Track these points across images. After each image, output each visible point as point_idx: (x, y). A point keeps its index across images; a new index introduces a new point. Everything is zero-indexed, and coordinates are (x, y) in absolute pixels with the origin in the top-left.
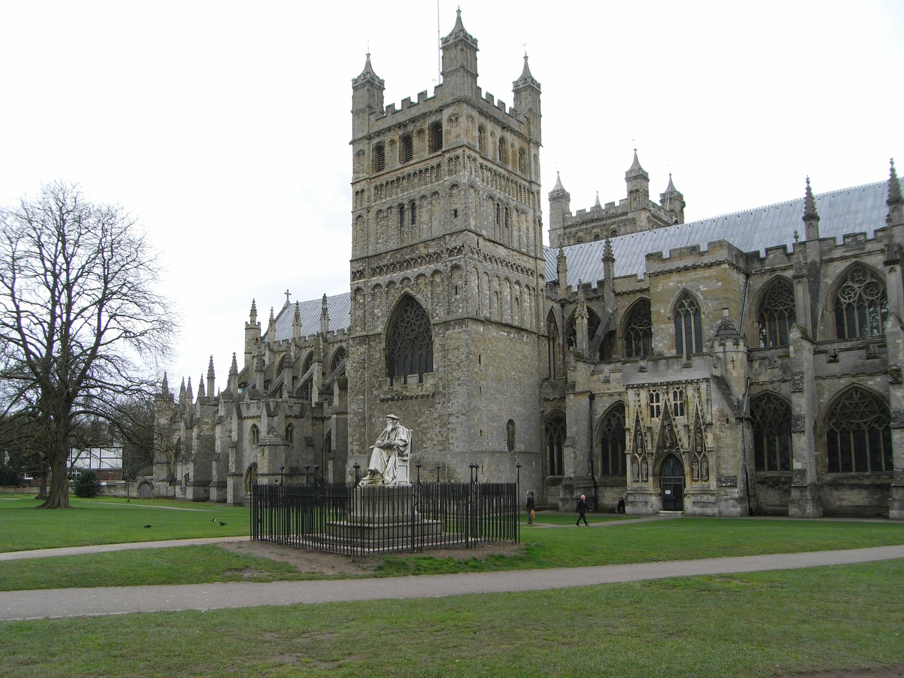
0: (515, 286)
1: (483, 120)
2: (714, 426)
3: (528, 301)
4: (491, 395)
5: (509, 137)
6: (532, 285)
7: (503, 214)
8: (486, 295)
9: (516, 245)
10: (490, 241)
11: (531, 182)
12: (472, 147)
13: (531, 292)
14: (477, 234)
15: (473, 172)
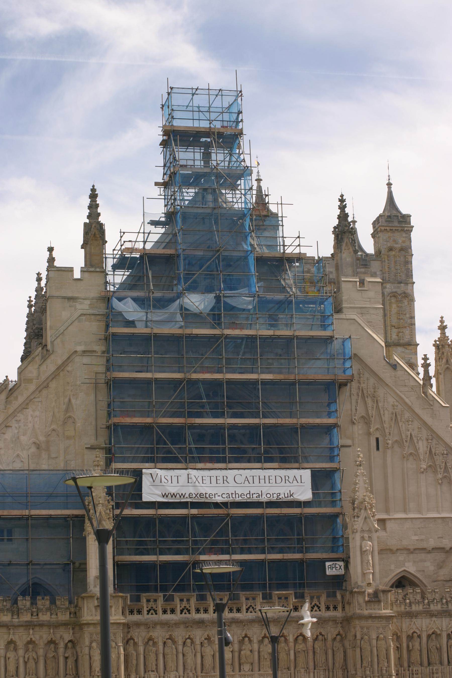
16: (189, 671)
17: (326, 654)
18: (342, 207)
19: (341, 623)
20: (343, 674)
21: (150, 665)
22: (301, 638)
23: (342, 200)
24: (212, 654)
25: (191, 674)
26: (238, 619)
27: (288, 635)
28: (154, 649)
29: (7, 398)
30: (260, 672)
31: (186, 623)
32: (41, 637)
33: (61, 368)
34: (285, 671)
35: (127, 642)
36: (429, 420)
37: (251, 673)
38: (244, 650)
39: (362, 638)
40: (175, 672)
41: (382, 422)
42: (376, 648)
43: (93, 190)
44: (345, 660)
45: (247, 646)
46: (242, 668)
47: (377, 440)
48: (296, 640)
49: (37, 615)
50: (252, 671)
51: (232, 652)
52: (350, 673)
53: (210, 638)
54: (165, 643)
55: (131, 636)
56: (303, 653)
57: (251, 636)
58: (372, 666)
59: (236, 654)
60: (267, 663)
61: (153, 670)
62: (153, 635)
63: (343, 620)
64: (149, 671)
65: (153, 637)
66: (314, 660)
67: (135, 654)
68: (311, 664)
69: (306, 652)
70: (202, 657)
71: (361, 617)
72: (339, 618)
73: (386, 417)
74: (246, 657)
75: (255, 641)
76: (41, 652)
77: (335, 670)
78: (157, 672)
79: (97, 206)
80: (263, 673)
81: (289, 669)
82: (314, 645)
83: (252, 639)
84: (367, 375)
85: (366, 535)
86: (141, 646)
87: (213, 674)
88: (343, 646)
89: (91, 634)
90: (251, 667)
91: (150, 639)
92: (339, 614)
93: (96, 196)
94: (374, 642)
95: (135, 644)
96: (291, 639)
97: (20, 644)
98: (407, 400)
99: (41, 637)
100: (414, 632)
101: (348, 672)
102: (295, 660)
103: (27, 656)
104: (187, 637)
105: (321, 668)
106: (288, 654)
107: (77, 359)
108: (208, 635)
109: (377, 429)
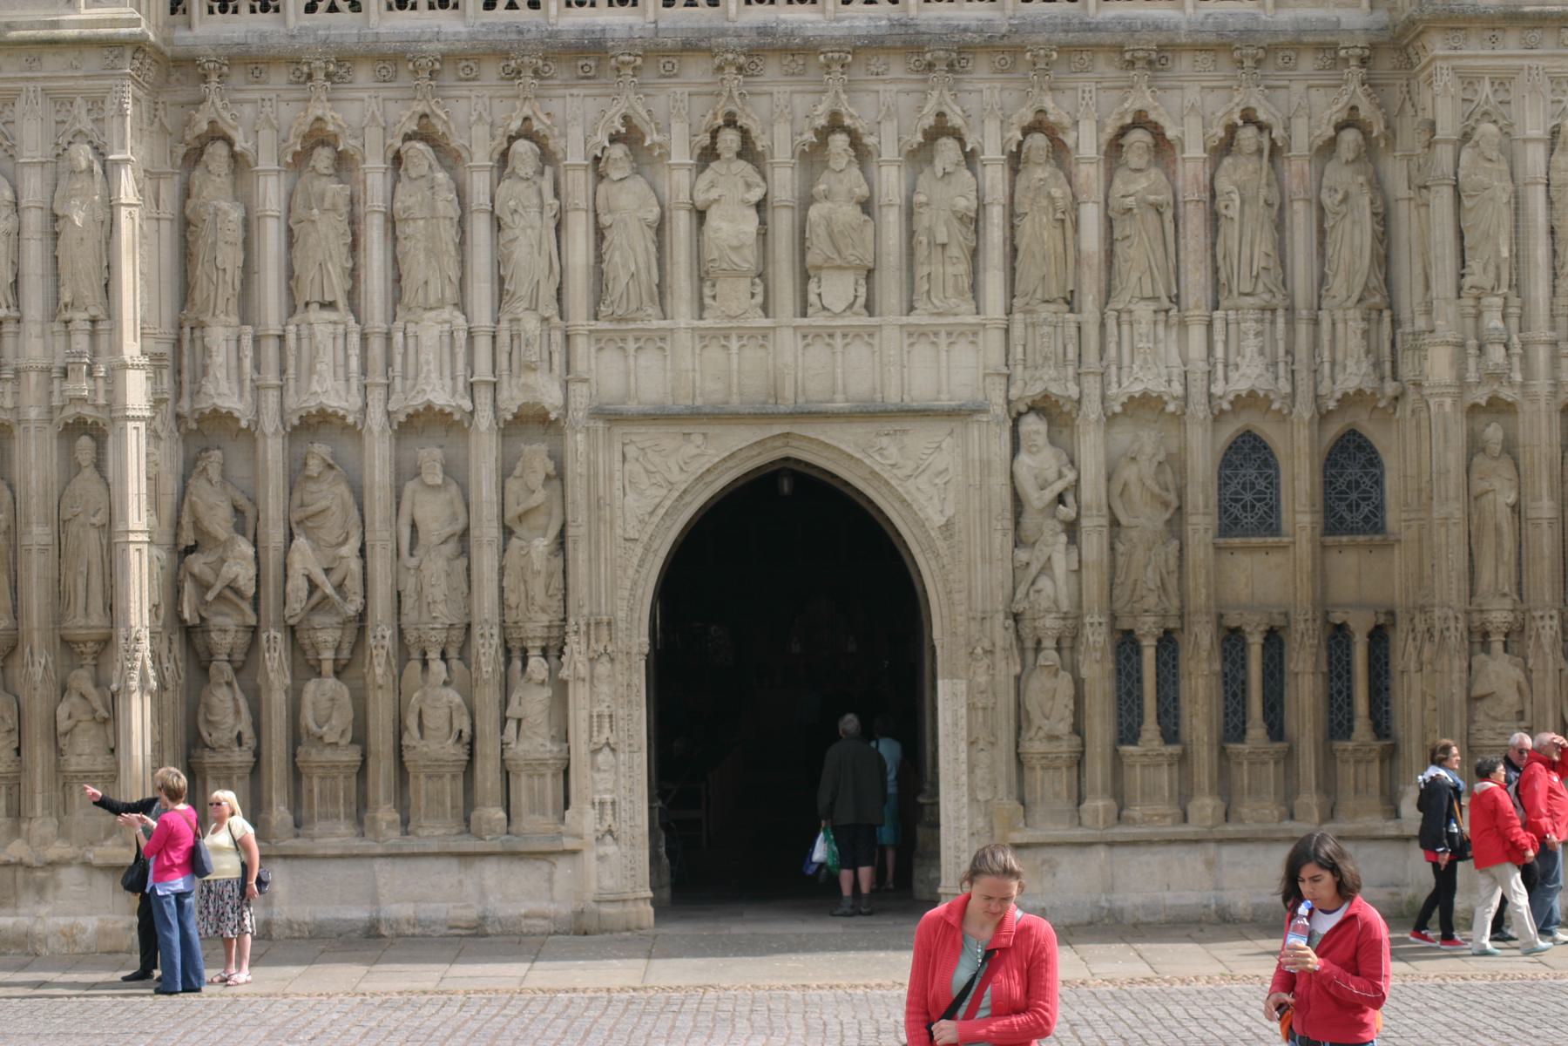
16: (519, 307)
17: (1280, 225)
19: (1363, 62)
20: (1366, 334)
21: (314, 272)
22: (1139, 137)
24: (653, 214)
25: (531, 324)
26: (791, 34)
27: (1067, 121)
28: (334, 190)
30: (912, 319)
31: (505, 55)
34: (1045, 312)
35: (194, 156)
37: (865, 320)
39: (1466, 137)
40: (447, 313)
42: (1541, 189)
44: (1384, 258)
45: (842, 177)
46: (812, 298)
48: (1115, 148)
50: (869, 308)
51: (760, 206)
52: (1407, 328)
53: (643, 137)
54: (397, 159)
55: (212, 123)
56: (1152, 217)
57: (861, 125)
58: (1517, 286)
59: (783, 223)
60: (950, 270)
61: (328, 298)
62: (329, 115)
63: (1373, 47)
64: (307, 304)
65: (331, 128)
66: (1214, 256)
67: (236, 215)
68: (1195, 281)
69: (1168, 215)
70: (600, 234)
72: (1351, 31)
74: (831, 235)
75: (889, 150)
77: (1325, 317)
78: (354, 309)
80: (926, 320)
81: (1071, 301)
82: (1212, 179)
83: (870, 140)
86: (267, 172)
87: (656, 324)
88: (1377, 184)
90: (862, 291)
91: (318, 138)
94: (1534, 158)
95: (238, 161)
96: (1087, 142)
101: (1395, 323)
102: (1110, 254)
104: (515, 125)
105: (1250, 300)
106: (1069, 222)
108: (626, 119)
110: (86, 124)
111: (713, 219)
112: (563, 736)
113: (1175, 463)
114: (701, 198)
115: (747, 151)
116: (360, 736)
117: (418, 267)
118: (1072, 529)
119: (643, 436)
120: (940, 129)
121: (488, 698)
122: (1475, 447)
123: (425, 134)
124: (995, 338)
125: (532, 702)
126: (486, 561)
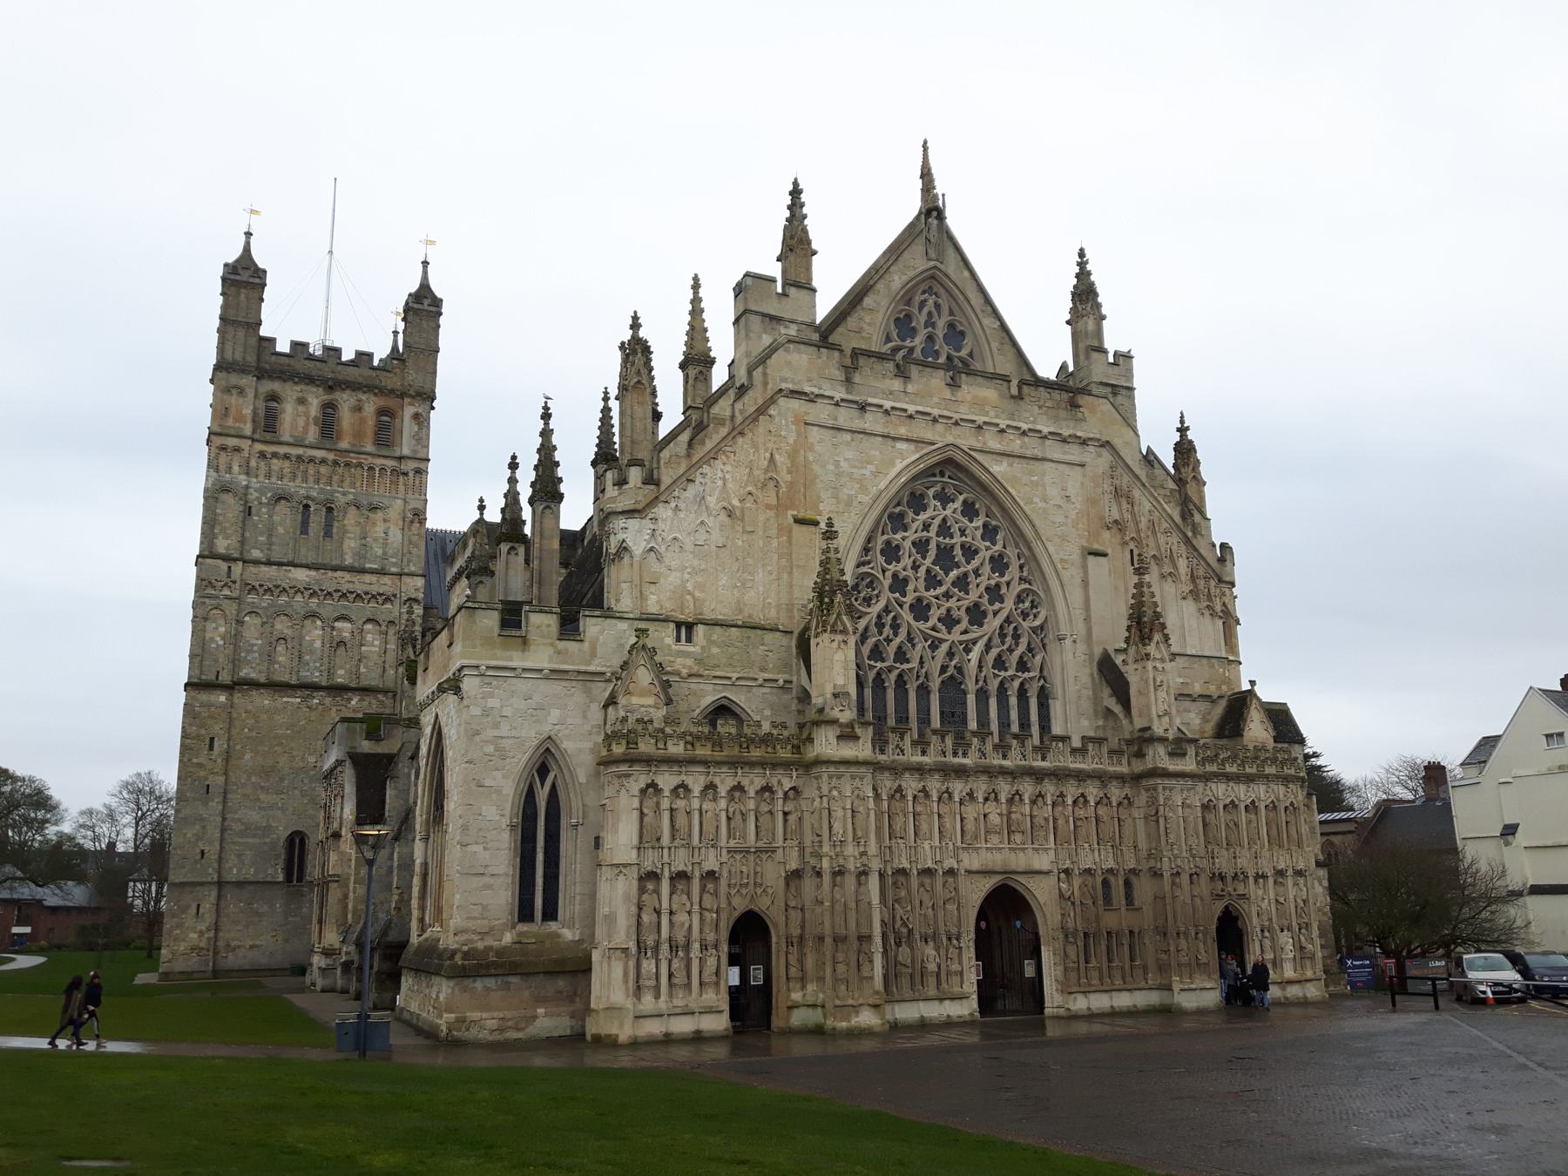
0: (336, 624)
1: (276, 386)
2: (343, 839)
3: (373, 641)
4: (245, 796)
5: (346, 400)
6: (380, 618)
7: (317, 520)
8: (253, 645)
9: (348, 561)
10: (269, 563)
11: (400, 458)
12: (233, 432)
13: (384, 628)
14: (225, 558)
15: (236, 468)
18: (1082, 264)
22: (1081, 799)
23: (1082, 254)
29: (691, 440)
32: (752, 782)
33: (762, 410)
36: (1190, 534)
38: (1015, 812)
41: (1138, 531)
43: (796, 183)
47: (1132, 551)
48: (1075, 802)
49: (748, 748)
54: (915, 797)
59: (1005, 818)
70: (962, 820)
71: (1166, 774)
73: (1143, 524)
76: (751, 805)
79: (802, 205)
84: (1120, 470)
85: (1159, 665)
89: (830, 777)
92: (1124, 769)
93: (801, 192)
97: (723, 790)
98: (1166, 506)
99: (752, 782)
100: (1210, 800)
103: (731, 810)
106: (1067, 822)
107: (782, 401)
109: (1132, 539)
110: (859, 786)
111: (991, 817)
112: (960, 963)
113: (1094, 888)
114: (987, 811)
115: (996, 799)
116: (913, 961)
117: (924, 827)
118: (1073, 903)
119: (976, 877)
120: (1040, 795)
121: (943, 952)
122: (1173, 883)
123: (924, 790)
124: (1052, 853)
125: (953, 952)
126: (941, 913)
